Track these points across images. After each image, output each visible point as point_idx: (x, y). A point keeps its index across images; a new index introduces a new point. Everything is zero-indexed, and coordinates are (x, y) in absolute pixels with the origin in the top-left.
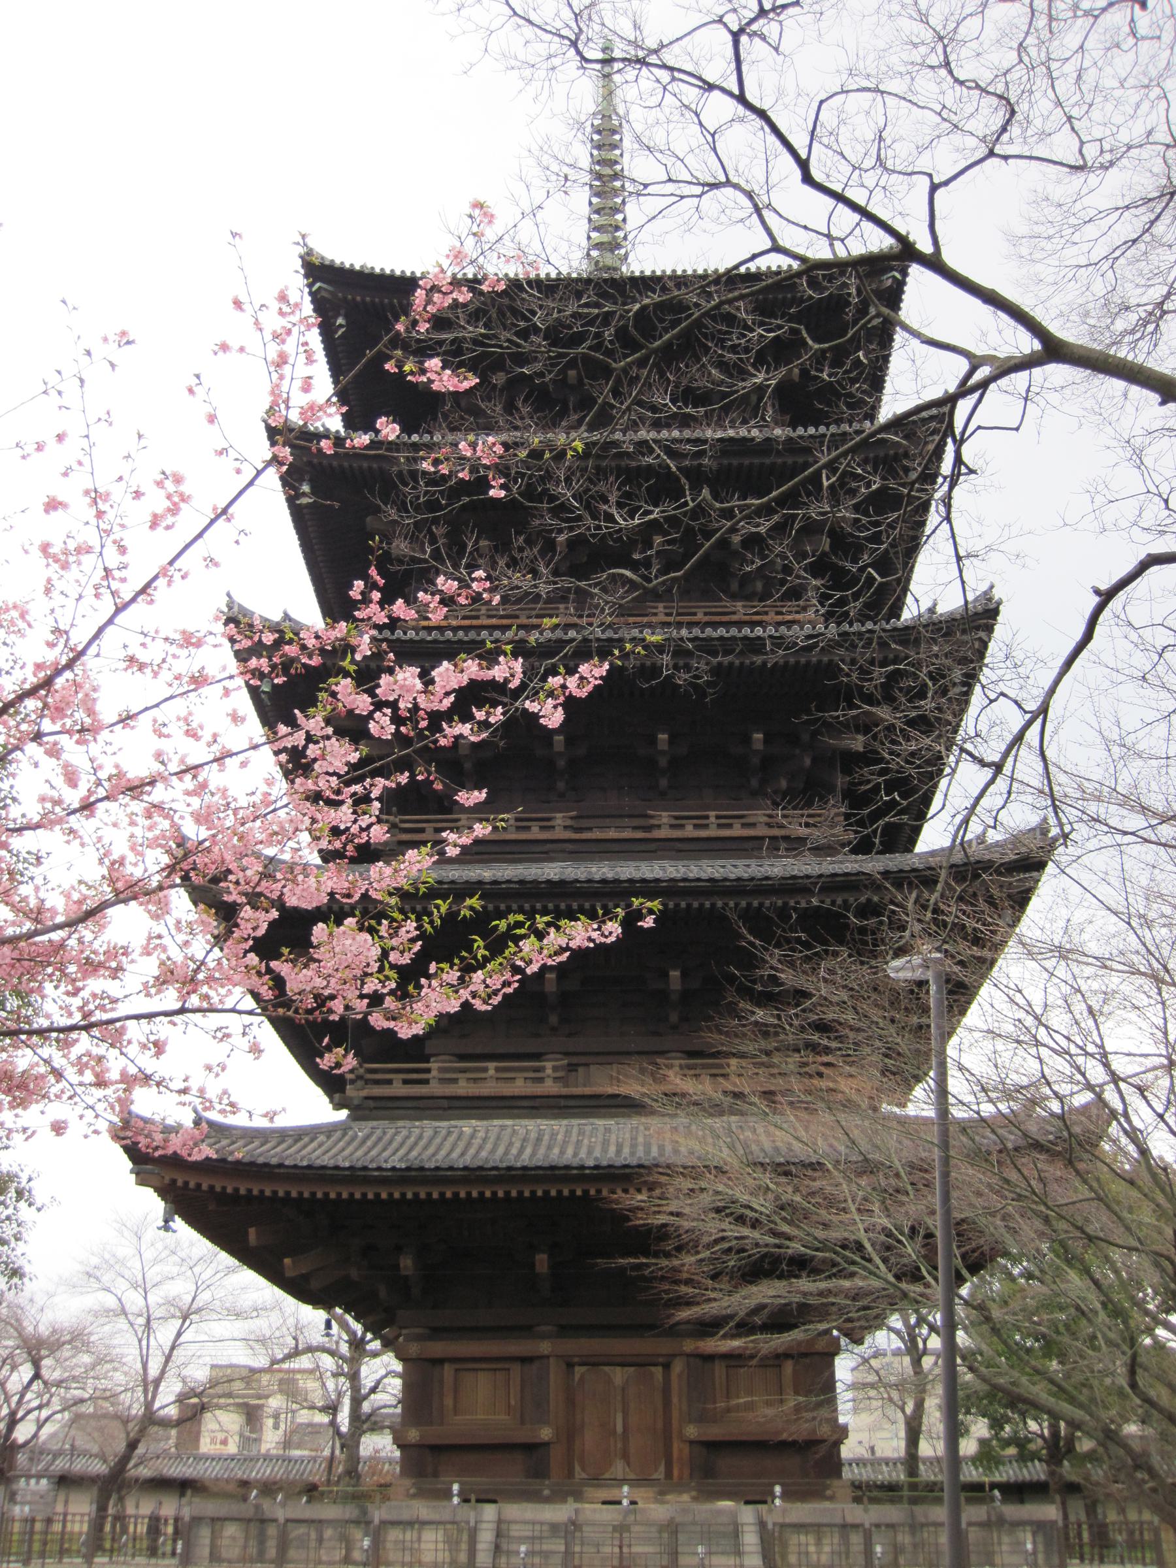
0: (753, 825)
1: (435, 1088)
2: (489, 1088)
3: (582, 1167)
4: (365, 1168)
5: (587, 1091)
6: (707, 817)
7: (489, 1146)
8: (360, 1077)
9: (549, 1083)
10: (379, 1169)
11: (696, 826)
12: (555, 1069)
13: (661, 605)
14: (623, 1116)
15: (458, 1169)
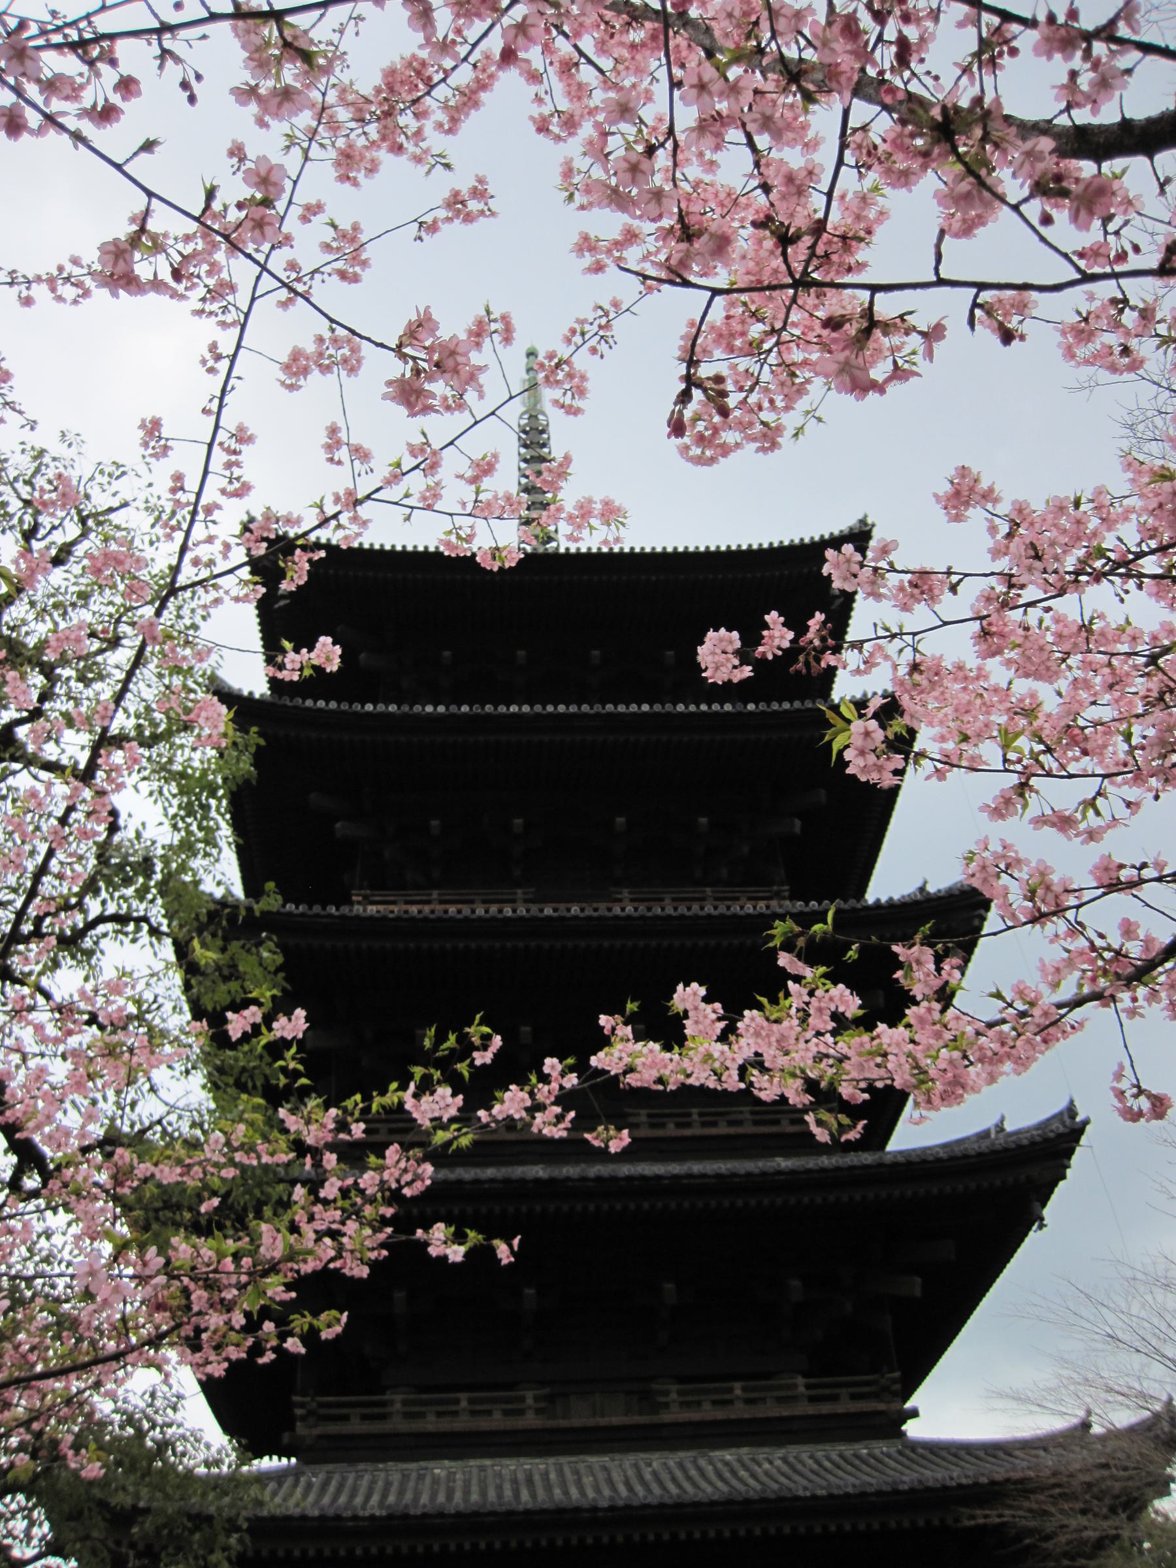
0: (739, 1123)
1: (398, 1424)
2: (462, 1424)
3: (595, 1509)
4: (338, 1518)
5: (576, 1422)
6: (689, 1115)
7: (475, 1488)
10: (355, 1518)
11: (679, 1125)
12: (536, 1399)
14: (619, 1451)
15: (450, 1516)
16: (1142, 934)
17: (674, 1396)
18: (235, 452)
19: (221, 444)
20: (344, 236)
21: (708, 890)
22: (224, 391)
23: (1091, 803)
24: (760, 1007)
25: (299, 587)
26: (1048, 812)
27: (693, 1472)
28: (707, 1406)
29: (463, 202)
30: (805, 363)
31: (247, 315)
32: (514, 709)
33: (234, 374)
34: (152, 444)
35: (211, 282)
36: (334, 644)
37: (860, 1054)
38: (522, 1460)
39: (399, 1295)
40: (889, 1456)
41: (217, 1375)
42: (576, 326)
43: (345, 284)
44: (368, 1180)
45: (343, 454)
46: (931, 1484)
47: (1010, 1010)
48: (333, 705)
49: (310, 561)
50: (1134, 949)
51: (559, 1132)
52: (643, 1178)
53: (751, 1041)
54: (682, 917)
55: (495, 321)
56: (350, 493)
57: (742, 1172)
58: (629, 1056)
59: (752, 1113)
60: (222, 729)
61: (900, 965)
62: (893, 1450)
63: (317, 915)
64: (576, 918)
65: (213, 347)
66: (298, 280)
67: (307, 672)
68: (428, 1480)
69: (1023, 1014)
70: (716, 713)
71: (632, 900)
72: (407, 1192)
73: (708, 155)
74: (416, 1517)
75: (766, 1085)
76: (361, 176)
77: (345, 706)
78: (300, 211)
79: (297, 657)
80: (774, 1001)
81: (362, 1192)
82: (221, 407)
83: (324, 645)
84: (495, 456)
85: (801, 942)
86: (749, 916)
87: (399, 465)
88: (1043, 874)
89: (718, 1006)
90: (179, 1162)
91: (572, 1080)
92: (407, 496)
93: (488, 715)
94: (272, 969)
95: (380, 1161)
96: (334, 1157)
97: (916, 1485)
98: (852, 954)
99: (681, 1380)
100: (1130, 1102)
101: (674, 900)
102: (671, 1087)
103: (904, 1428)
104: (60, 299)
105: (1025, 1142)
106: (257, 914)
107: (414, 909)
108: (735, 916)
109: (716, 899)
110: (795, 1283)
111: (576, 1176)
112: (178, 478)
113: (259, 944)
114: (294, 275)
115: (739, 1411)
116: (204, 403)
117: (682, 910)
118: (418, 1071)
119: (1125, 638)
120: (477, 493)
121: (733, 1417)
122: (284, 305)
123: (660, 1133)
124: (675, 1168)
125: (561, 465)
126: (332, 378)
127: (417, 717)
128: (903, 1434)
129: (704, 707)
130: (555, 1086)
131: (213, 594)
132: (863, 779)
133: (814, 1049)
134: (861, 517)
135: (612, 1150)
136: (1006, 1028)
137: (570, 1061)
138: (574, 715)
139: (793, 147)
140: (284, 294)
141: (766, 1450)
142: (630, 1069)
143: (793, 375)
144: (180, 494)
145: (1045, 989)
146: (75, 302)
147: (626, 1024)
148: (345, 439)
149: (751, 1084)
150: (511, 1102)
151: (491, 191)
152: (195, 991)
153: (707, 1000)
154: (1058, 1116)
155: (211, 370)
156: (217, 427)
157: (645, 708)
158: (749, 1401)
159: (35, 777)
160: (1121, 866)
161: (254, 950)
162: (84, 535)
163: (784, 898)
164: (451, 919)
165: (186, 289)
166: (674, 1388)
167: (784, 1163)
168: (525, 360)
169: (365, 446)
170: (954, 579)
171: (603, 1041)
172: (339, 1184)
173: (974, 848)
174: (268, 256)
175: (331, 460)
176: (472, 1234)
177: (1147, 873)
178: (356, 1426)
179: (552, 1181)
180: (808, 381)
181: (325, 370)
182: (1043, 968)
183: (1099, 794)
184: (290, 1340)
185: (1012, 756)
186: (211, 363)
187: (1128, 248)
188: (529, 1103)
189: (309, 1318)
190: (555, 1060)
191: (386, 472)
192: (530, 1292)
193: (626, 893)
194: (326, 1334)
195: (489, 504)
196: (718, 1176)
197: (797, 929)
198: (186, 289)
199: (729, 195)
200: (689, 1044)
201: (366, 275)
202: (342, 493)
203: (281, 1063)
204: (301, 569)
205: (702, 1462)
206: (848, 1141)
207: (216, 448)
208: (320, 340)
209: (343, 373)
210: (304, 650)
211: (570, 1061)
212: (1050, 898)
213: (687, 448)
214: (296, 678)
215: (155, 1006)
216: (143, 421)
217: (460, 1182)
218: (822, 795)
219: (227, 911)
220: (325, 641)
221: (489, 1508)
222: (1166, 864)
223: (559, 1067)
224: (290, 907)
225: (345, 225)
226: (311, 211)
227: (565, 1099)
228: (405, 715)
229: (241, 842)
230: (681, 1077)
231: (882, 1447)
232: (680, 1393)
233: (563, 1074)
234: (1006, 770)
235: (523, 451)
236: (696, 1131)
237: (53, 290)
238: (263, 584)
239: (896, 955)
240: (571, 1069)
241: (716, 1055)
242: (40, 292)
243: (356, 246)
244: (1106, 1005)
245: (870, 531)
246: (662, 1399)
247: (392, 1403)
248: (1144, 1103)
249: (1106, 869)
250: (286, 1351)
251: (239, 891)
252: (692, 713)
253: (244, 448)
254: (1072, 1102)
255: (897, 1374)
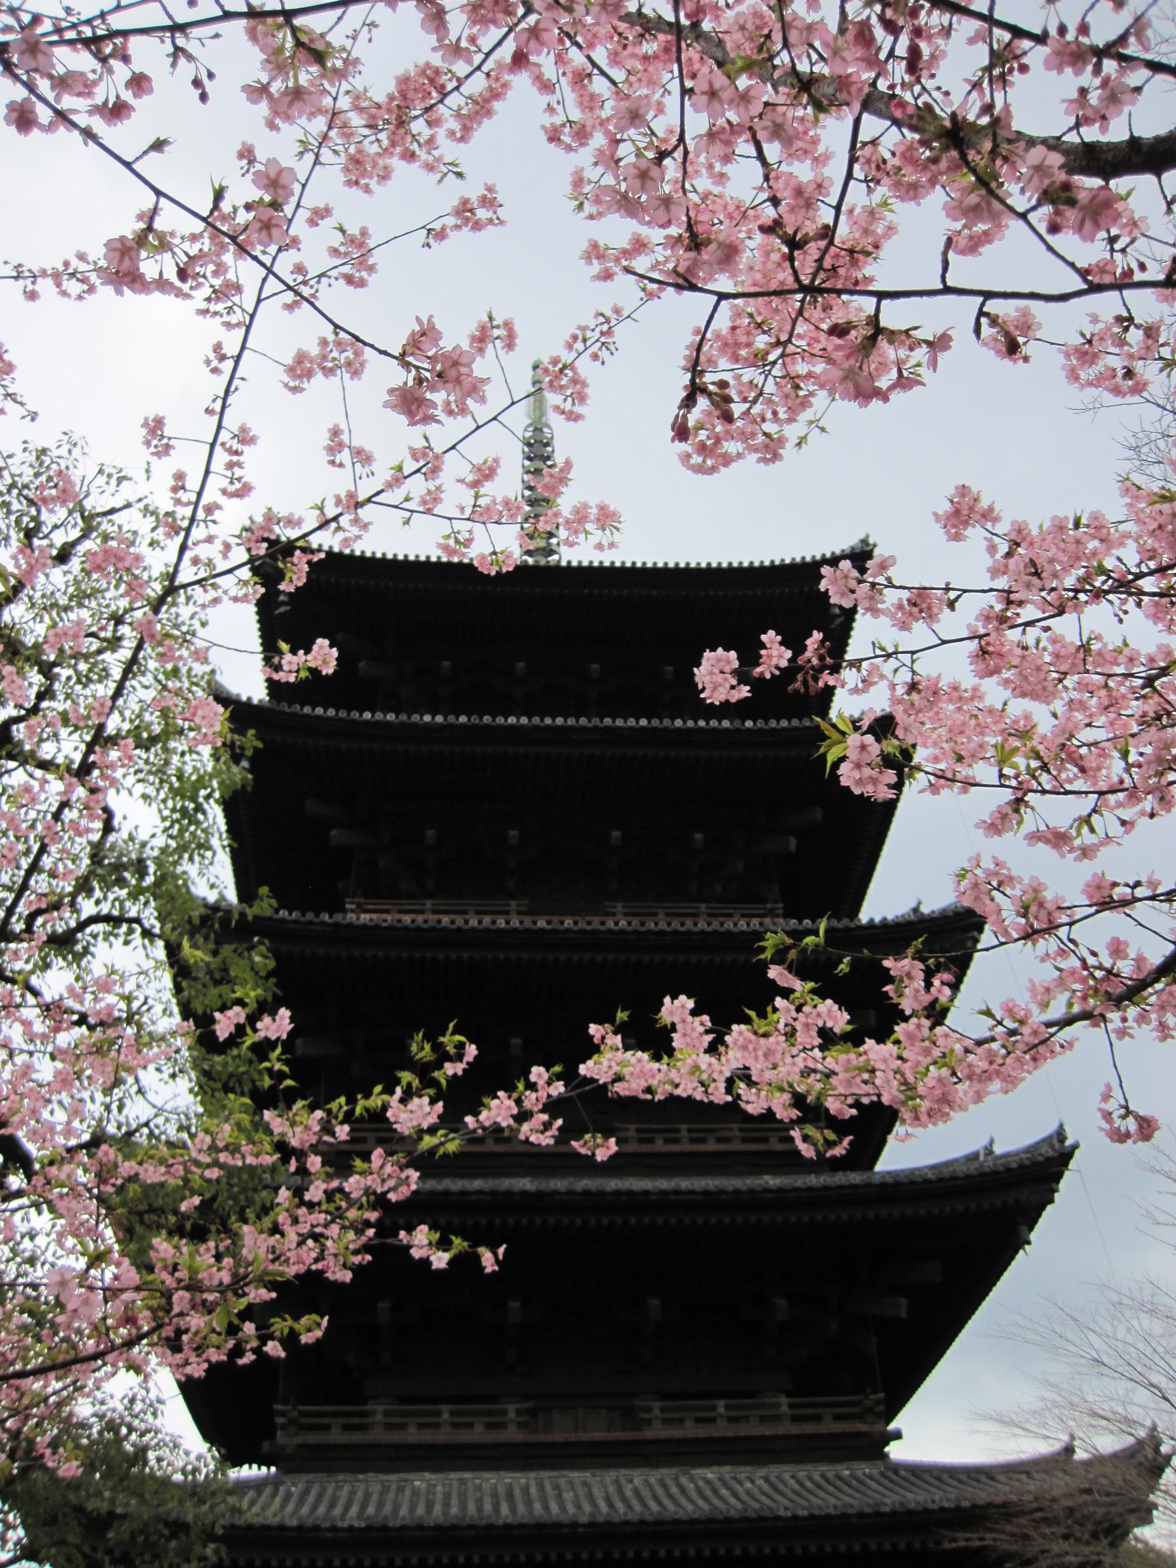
0: (728, 1140)
1: (379, 1435)
2: (442, 1436)
3: (574, 1525)
4: (316, 1528)
5: (557, 1437)
6: (678, 1131)
7: (454, 1502)
8: (292, 1422)
9: (512, 1429)
10: (334, 1528)
11: (667, 1141)
12: (519, 1413)
13: (619, 905)
15: (428, 1528)
16: (1132, 954)
17: (657, 1412)
18: (237, 453)
19: (223, 444)
20: (352, 241)
21: (703, 906)
22: (227, 392)
23: (1086, 820)
24: (747, 1021)
25: (298, 589)
26: (1043, 828)
27: (674, 1490)
28: (689, 1423)
29: (471, 211)
30: (810, 375)
31: (252, 316)
32: (512, 720)
33: (238, 375)
34: (154, 442)
35: (217, 282)
36: (331, 646)
37: (847, 1070)
38: (503, 1474)
39: (383, 1306)
40: (871, 1478)
41: (196, 1375)
42: (578, 332)
43: (351, 288)
44: (354, 1184)
45: (345, 456)
46: (913, 1506)
47: (1000, 1029)
48: (331, 712)
49: (309, 563)
50: (1126, 968)
51: (546, 1140)
52: (630, 1193)
53: (739, 1055)
54: (676, 932)
55: (498, 327)
56: (351, 495)
57: (730, 1189)
58: (615, 1063)
59: (741, 1130)
60: (218, 728)
61: (891, 980)
62: (875, 1472)
63: (310, 923)
64: (568, 931)
65: (218, 348)
66: (305, 283)
67: (304, 674)
68: (408, 1492)
69: (1012, 1033)
70: (714, 729)
71: (626, 914)
72: (392, 1197)
73: (718, 167)
74: (394, 1529)
75: (753, 1098)
76: (373, 183)
77: (343, 714)
78: (308, 214)
79: (295, 659)
80: (763, 1015)
81: (346, 1196)
82: (224, 407)
83: (321, 647)
84: (496, 461)
85: (792, 954)
86: (742, 933)
87: (400, 469)
88: (1036, 891)
89: (706, 1018)
90: (162, 1161)
91: (559, 1088)
92: (407, 499)
93: (487, 726)
94: (263, 973)
95: (366, 1166)
96: (318, 1159)
97: (898, 1507)
98: (844, 967)
99: (664, 1396)
100: (1118, 1122)
101: (667, 915)
102: (659, 1097)
103: (886, 1449)
104: (64, 293)
105: (1014, 1165)
106: (250, 918)
107: (407, 919)
108: (729, 932)
109: (710, 915)
110: (781, 1302)
111: (563, 1190)
112: (180, 477)
113: (251, 948)
114: (300, 278)
115: (722, 1429)
116: (207, 403)
117: (676, 925)
118: (406, 1076)
119: (1121, 659)
120: (477, 497)
121: (715, 1435)
122: (290, 307)
123: (646, 1148)
124: (663, 1184)
125: (562, 470)
126: (334, 381)
127: (415, 726)
128: (885, 1456)
129: (702, 723)
130: (543, 1094)
131: (212, 594)
132: (857, 791)
133: (801, 1065)
134: (862, 536)
135: (599, 1159)
136: (995, 1046)
137: (557, 1069)
138: (571, 728)
139: (802, 162)
140: (289, 297)
141: (749, 1469)
142: (618, 1078)
143: (798, 387)
144: (181, 494)
145: (1035, 1009)
146: (80, 298)
147: (615, 1033)
148: (347, 441)
149: (739, 1096)
150: (498, 1110)
151: (500, 198)
152: (186, 993)
153: (694, 1013)
154: (1048, 1140)
155: (215, 371)
156: (219, 427)
157: (643, 722)
158: (731, 1420)
159: (31, 776)
160: (1115, 884)
161: (246, 954)
162: (85, 536)
163: (778, 916)
164: (444, 929)
165: (191, 288)
166: (658, 1404)
167: (772, 1181)
168: (531, 373)
169: (367, 449)
170: (952, 595)
171: (591, 1049)
172: (324, 1186)
173: (967, 866)
174: (274, 259)
175: (332, 463)
176: (457, 1241)
177: (1140, 892)
178: (336, 1436)
179: (539, 1195)
180: (812, 394)
181: (329, 372)
182: (1033, 990)
183: (1094, 811)
184: (270, 1344)
185: (1006, 771)
186: (215, 363)
187: (1134, 266)
188: (515, 1111)
189: (290, 1322)
190: (542, 1069)
191: (388, 475)
192: (514, 1304)
193: (619, 907)
194: (306, 1339)
195: (488, 509)
196: (706, 1193)
197: (789, 941)
198: (191, 288)
199: (738, 207)
200: (677, 1054)
201: (372, 280)
202: (343, 496)
203: (266, 1064)
204: (300, 570)
205: (684, 1480)
206: (834, 1157)
207: (218, 448)
208: (324, 342)
209: (347, 376)
210: (301, 652)
211: (557, 1069)
212: (1043, 915)
213: (689, 456)
214: (292, 679)
215: (145, 1008)
216: (146, 419)
217: (446, 1193)
218: (818, 813)
219: (220, 914)
220: (322, 643)
221: (468, 1521)
222: (1159, 883)
223: (546, 1076)
224: (284, 913)
225: (353, 230)
226: (319, 215)
227: (552, 1107)
228: (402, 724)
229: (235, 845)
230: (668, 1088)
231: (864, 1469)
232: (663, 1410)
233: (549, 1083)
234: (1002, 786)
235: (527, 463)
236: (685, 1147)
237: (59, 285)
238: (263, 585)
239: (888, 970)
240: (559, 1077)
241: (704, 1067)
242: (45, 286)
243: (364, 251)
244: (1097, 1025)
245: (871, 551)
246: (643, 1415)
247: (374, 1413)
248: (1131, 1124)
249: (1099, 887)
250: (266, 1354)
251: (232, 896)
252: (690, 729)
253: (246, 448)
254: (1061, 1126)
255: (881, 1395)
